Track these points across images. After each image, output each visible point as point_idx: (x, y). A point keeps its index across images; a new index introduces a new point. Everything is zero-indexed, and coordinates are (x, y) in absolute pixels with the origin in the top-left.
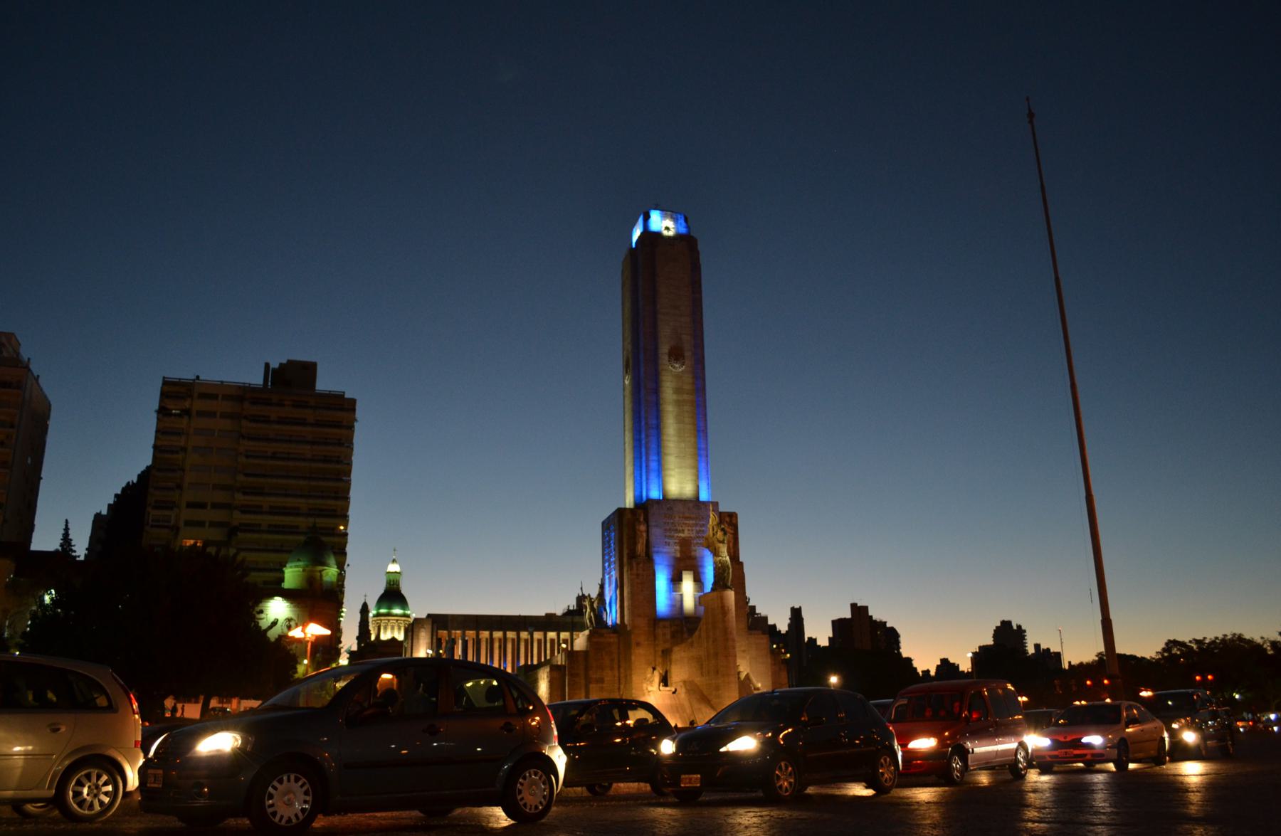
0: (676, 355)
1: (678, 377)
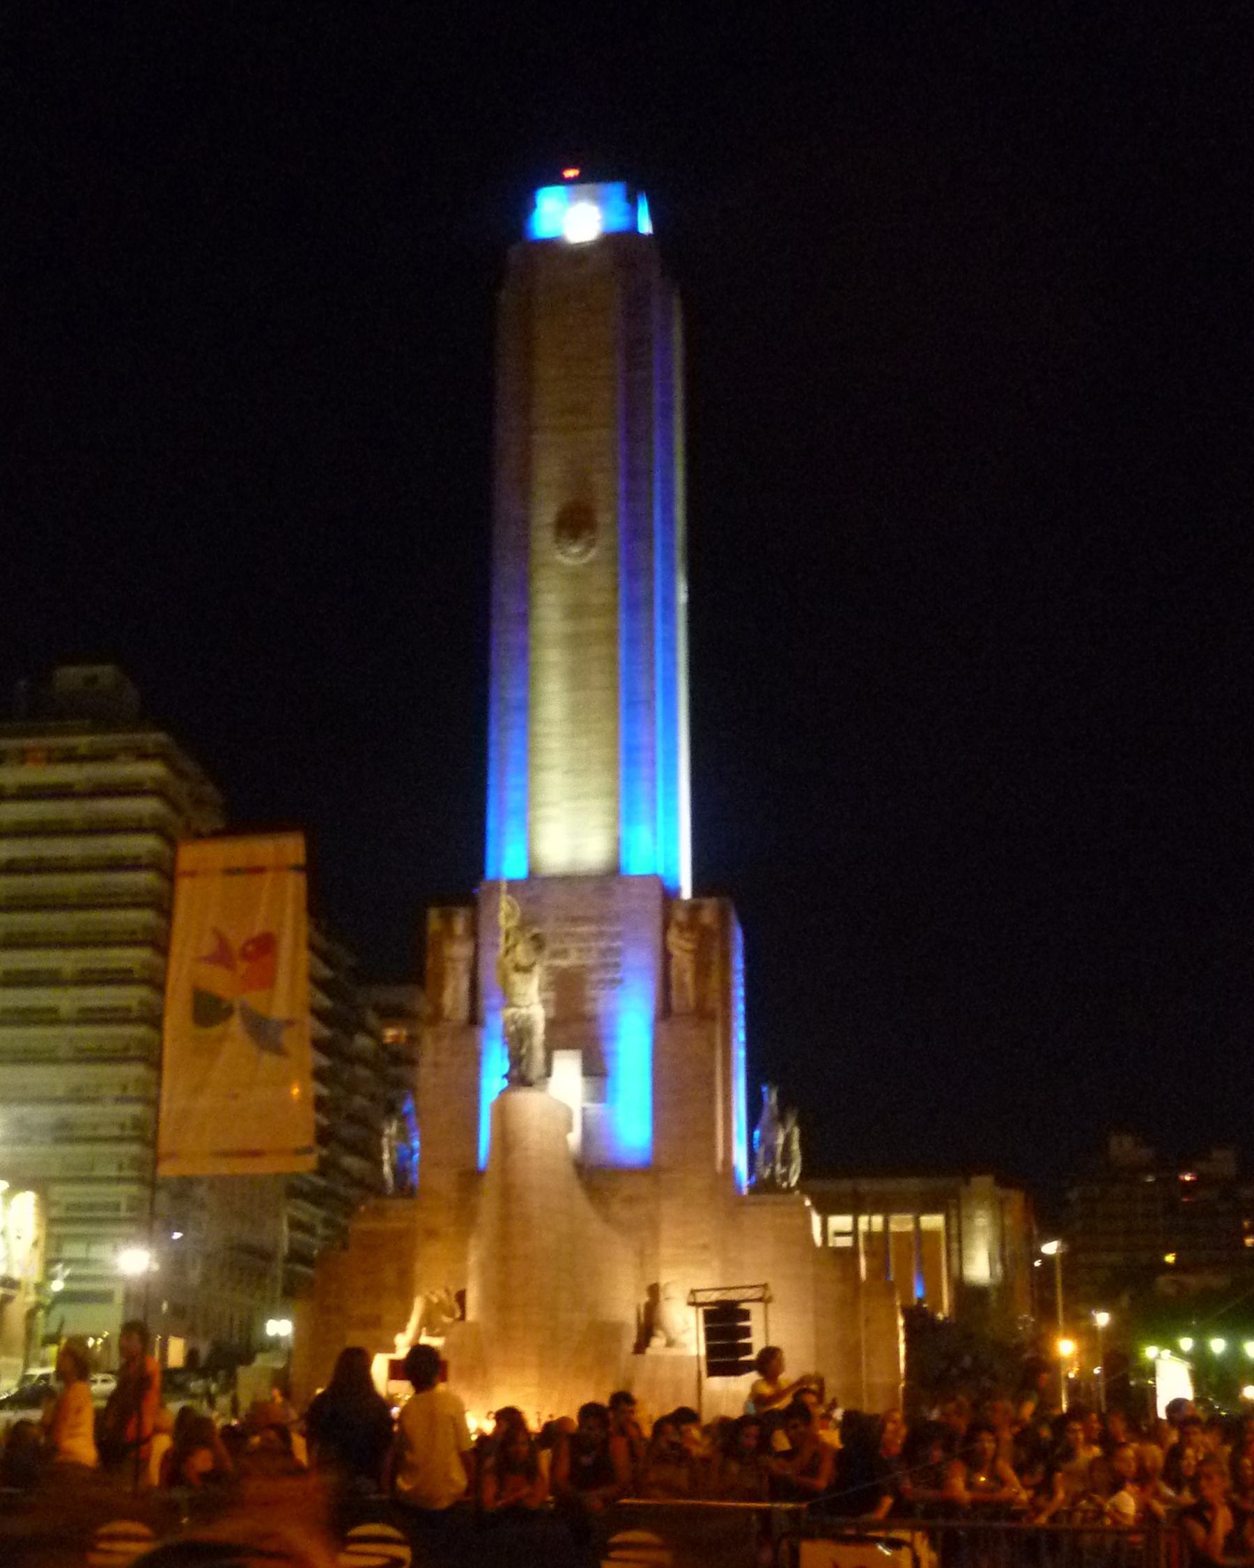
0: (575, 523)
1: (576, 577)
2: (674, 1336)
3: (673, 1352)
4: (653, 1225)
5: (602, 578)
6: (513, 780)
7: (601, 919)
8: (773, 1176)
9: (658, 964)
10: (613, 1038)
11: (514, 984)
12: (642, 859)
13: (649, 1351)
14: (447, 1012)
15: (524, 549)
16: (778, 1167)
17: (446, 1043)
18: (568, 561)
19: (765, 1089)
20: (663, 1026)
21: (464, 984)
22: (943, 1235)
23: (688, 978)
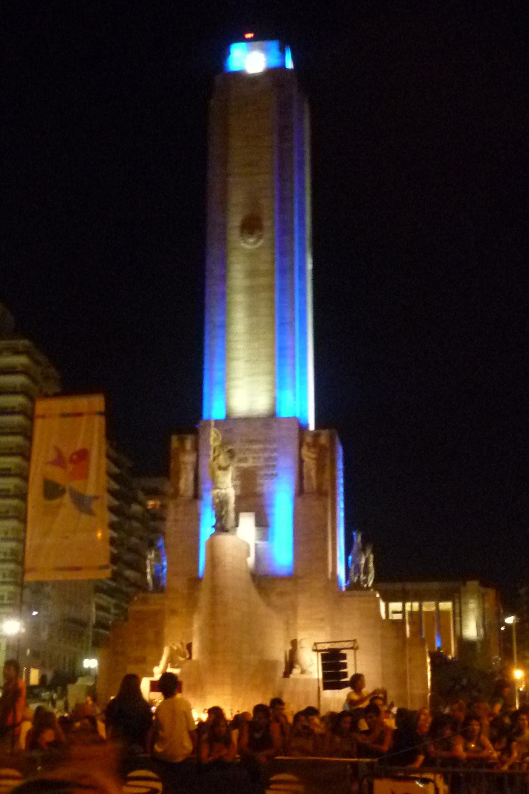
0: (251, 226)
2: (305, 668)
3: (305, 676)
4: (294, 607)
5: (266, 256)
6: (218, 365)
7: (266, 441)
8: (359, 581)
9: (297, 465)
10: (272, 506)
11: (218, 477)
12: (287, 410)
13: (292, 676)
14: (181, 492)
15: (223, 240)
16: (362, 576)
17: (181, 508)
18: (248, 247)
19: (354, 534)
20: (299, 499)
21: (191, 477)
22: (451, 613)
23: (313, 473)
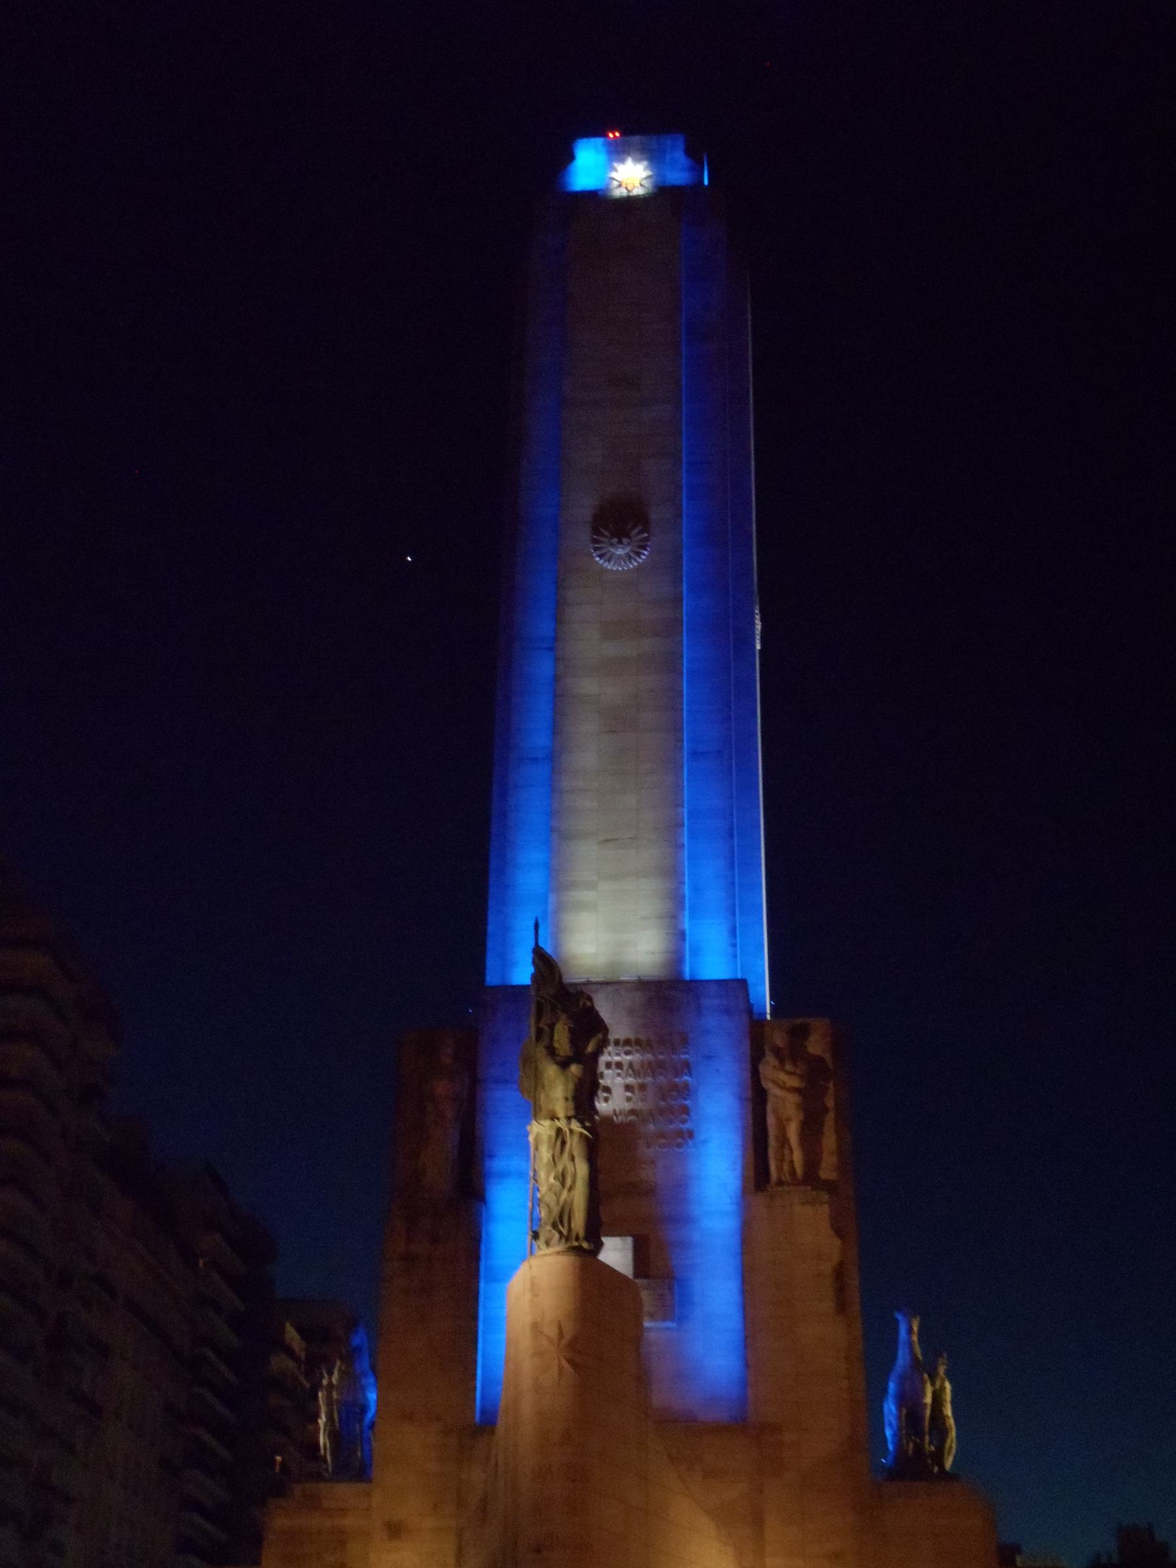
0: (620, 519)
12: (713, 963)
23: (793, 1131)
